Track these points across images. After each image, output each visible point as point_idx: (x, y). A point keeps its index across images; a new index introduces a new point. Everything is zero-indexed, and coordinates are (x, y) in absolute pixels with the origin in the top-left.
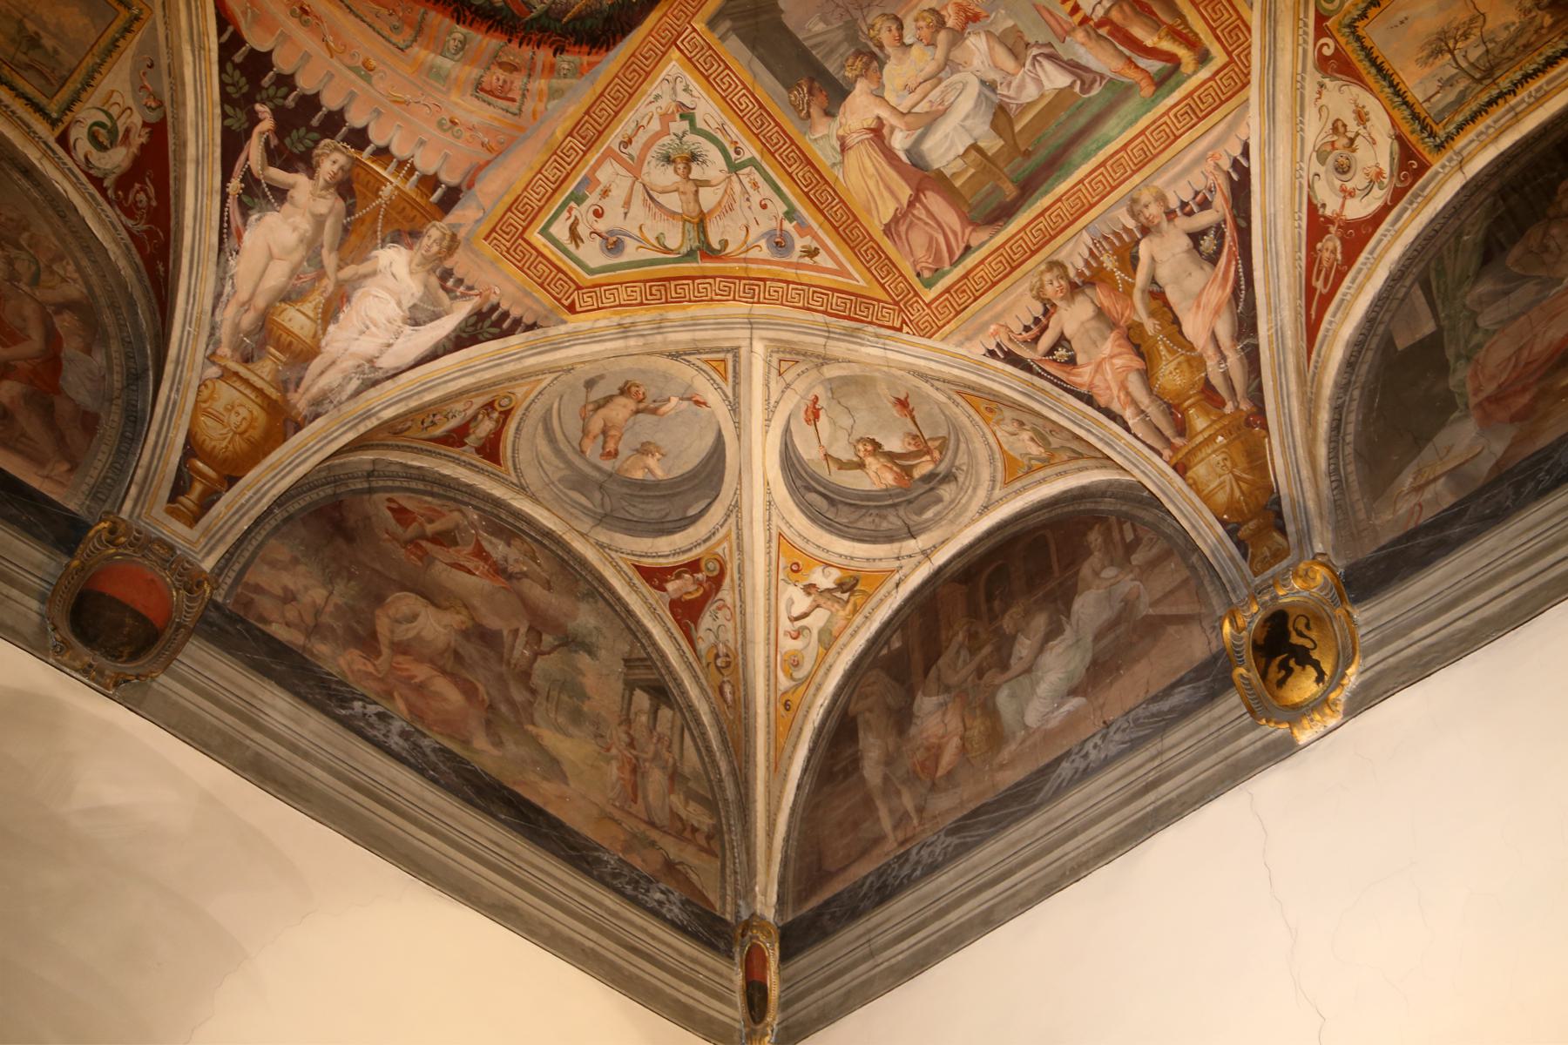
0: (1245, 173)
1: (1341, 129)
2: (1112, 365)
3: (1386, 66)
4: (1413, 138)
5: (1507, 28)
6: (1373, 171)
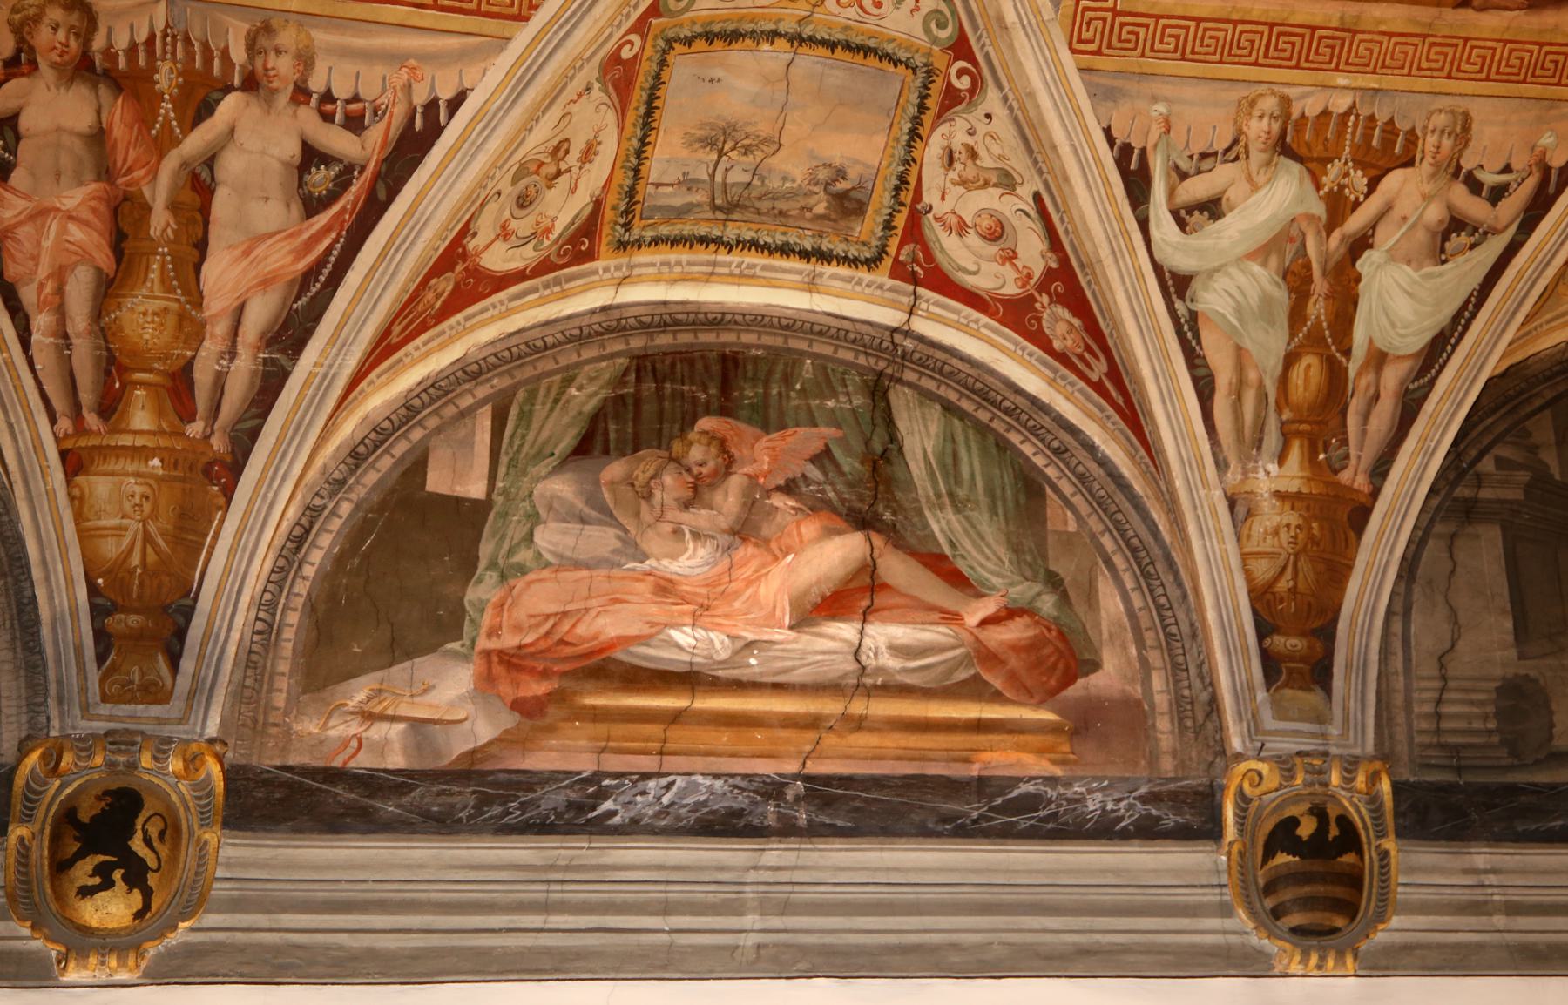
0: (434, 130)
1: (561, 154)
2: (63, 230)
3: (657, 115)
4: (609, 214)
6: (547, 223)
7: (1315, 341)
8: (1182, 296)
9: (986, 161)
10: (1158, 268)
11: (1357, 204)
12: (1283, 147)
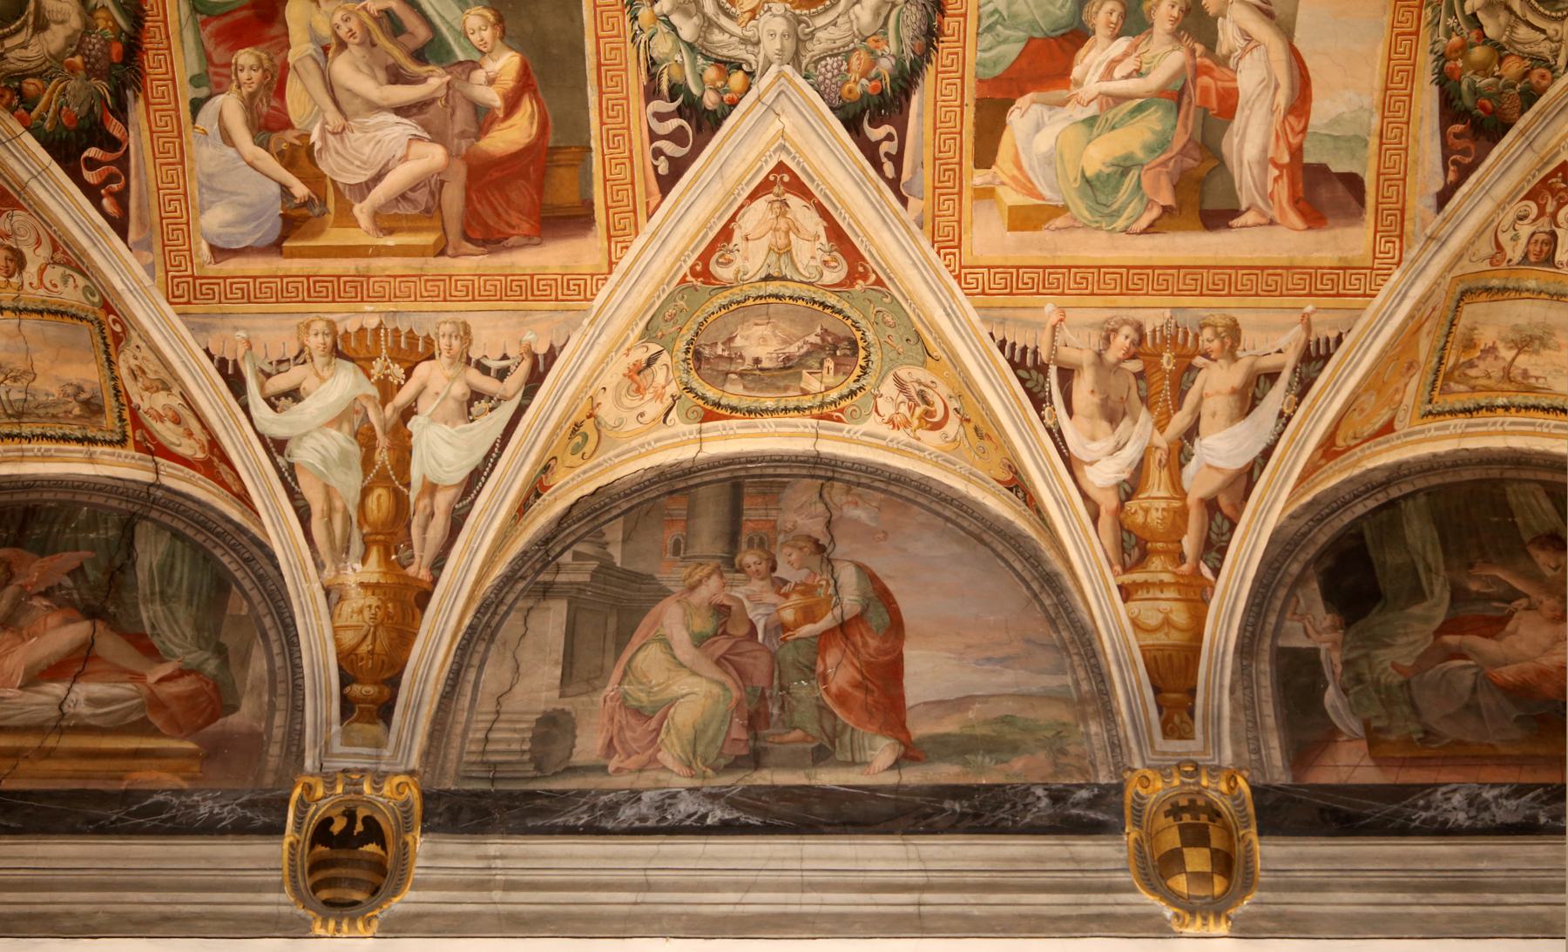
5: (47, 395)
7: (383, 478)
8: (281, 453)
9: (151, 376)
10: (261, 437)
11: (400, 387)
12: (338, 352)
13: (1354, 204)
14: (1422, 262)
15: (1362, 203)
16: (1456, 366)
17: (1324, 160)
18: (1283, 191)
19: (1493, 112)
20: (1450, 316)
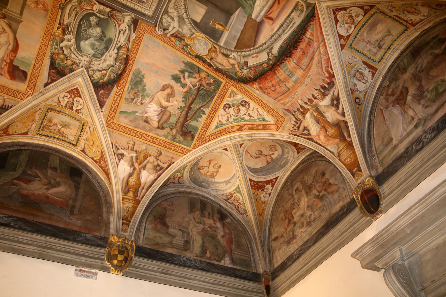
13: (24, 78)
14: (37, 97)
15: (26, 78)
16: (46, 125)
17: (18, 65)
18: (6, 69)
19: (63, 70)
20: (45, 113)
